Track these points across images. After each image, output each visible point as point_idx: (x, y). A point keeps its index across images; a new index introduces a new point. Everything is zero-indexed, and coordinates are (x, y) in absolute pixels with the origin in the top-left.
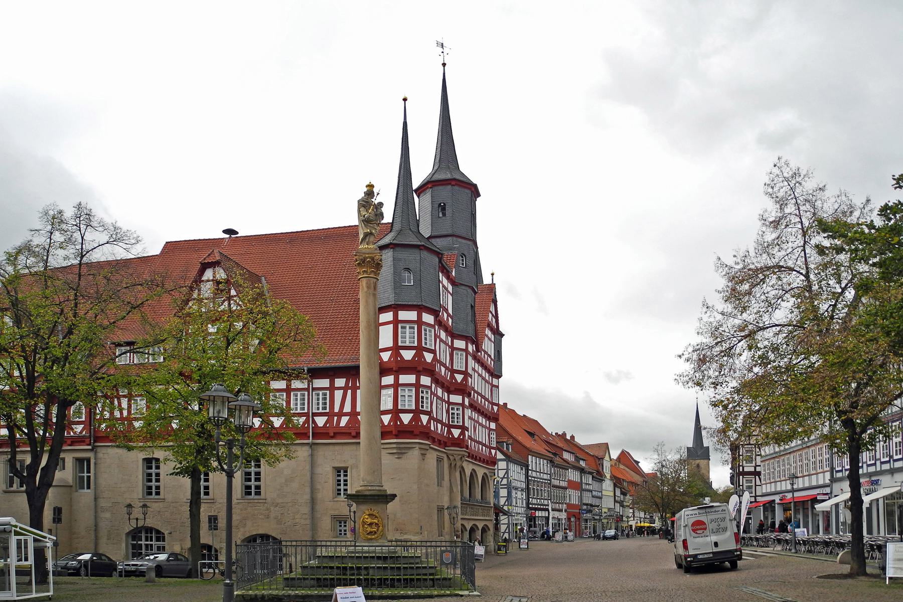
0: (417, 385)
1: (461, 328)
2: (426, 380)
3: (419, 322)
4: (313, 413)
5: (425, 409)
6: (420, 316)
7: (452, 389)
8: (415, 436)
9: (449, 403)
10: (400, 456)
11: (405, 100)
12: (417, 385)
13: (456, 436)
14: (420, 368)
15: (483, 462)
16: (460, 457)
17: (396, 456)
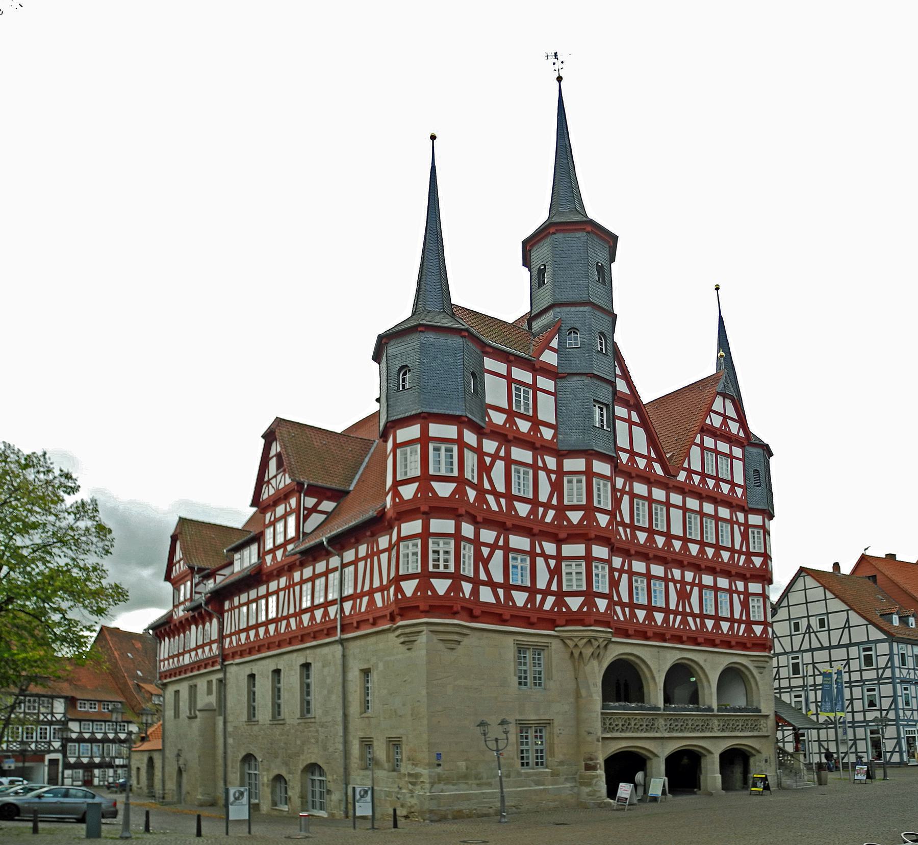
1: (573, 439)
7: (563, 535)
8: (427, 613)
9: (559, 558)
10: (409, 646)
11: (433, 138)
17: (407, 647)
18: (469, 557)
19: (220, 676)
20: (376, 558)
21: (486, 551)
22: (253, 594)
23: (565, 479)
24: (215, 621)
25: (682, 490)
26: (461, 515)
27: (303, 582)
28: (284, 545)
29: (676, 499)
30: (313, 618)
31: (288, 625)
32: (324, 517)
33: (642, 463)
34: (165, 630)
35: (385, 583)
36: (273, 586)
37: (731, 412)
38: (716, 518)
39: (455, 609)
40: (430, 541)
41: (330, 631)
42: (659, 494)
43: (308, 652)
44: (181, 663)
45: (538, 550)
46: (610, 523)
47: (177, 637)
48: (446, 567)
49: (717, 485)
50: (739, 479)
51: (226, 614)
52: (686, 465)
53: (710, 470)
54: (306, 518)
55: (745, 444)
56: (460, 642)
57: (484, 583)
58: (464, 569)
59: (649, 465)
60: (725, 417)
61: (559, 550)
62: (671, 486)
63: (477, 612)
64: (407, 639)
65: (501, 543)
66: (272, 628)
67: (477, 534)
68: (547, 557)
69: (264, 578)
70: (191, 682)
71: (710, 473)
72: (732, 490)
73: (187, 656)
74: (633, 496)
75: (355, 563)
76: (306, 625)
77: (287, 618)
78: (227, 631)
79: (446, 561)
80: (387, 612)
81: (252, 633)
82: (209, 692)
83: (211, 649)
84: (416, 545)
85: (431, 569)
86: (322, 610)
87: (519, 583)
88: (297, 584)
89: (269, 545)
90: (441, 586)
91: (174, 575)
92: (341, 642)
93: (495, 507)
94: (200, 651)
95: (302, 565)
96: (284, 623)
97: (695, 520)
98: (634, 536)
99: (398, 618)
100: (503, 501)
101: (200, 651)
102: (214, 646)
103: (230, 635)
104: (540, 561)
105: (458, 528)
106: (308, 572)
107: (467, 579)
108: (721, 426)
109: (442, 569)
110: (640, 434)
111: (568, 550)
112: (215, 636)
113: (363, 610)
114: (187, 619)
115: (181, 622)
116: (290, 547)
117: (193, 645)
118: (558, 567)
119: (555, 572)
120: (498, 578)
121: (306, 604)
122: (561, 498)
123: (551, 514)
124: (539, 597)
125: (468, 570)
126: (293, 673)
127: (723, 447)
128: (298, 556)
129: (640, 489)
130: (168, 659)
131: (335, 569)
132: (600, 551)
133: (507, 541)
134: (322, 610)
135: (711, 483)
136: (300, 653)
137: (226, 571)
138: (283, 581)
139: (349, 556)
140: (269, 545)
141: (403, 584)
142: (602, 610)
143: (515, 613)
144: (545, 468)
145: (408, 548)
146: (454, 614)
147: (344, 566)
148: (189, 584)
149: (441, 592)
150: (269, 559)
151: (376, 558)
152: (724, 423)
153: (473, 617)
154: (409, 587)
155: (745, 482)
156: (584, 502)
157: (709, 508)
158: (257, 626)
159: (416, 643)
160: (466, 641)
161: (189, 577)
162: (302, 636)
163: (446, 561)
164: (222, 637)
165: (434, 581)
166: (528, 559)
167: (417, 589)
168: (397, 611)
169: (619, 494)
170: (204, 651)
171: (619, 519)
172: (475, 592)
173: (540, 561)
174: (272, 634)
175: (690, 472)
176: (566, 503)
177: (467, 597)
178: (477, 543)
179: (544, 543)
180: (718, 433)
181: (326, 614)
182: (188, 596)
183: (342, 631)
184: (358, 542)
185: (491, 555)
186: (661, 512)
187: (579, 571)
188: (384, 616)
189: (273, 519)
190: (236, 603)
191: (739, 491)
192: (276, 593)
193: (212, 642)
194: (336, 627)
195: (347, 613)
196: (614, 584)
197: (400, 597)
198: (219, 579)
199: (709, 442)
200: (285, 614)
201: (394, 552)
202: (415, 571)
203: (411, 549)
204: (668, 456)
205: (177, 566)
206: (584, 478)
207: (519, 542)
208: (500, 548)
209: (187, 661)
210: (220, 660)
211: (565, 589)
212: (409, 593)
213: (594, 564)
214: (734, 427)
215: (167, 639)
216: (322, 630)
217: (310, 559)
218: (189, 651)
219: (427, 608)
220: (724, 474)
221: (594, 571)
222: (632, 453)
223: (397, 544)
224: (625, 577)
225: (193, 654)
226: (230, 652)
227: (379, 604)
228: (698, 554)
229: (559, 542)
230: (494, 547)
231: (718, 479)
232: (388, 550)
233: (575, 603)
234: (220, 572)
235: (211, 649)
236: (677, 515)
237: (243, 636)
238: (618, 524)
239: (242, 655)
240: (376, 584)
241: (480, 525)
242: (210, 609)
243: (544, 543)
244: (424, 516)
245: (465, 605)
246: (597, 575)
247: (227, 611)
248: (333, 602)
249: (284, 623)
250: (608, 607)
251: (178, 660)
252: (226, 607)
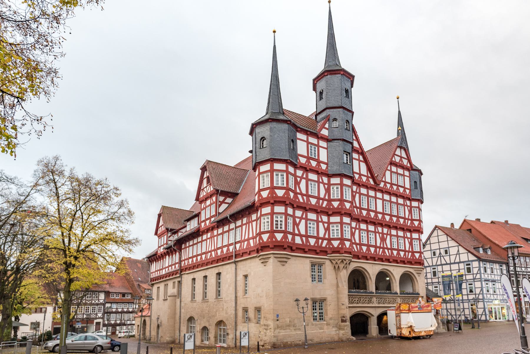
3: (272, 171)
4: (235, 242)
7: (330, 213)
8: (272, 249)
9: (329, 223)
10: (265, 264)
12: (272, 213)
13: (336, 246)
14: (272, 201)
15: (403, 262)
16: (340, 261)
18: (291, 223)
19: (179, 279)
20: (250, 224)
21: (298, 220)
22: (195, 241)
23: (331, 187)
24: (177, 253)
25: (382, 191)
26: (287, 205)
27: (218, 235)
28: (210, 218)
29: (379, 195)
30: (222, 251)
31: (211, 255)
32: (227, 205)
33: (364, 179)
34: (154, 258)
35: (254, 235)
36: (205, 237)
37: (404, 155)
38: (397, 204)
39: (285, 247)
40: (274, 216)
41: (230, 258)
42: (372, 193)
43: (220, 267)
44: (161, 274)
45: (320, 220)
46: (350, 207)
47: (159, 262)
48: (281, 228)
49: (398, 189)
50: (407, 186)
51: (183, 250)
52: (384, 180)
53: (395, 181)
54: (220, 206)
55: (410, 169)
56: (286, 262)
57: (297, 235)
58: (289, 228)
59: (368, 180)
60: (401, 157)
61: (329, 219)
62: (377, 189)
63: (294, 248)
64: (264, 261)
65: (304, 217)
66: (204, 256)
67: (294, 213)
68: (323, 223)
69: (201, 233)
70: (166, 283)
71: (394, 183)
72: (404, 191)
73: (164, 270)
74: (360, 194)
75: (241, 226)
76: (219, 255)
77: (211, 252)
78: (183, 258)
79: (281, 225)
80: (255, 249)
81: (195, 259)
82: (174, 287)
83: (175, 267)
84: (268, 218)
85: (275, 229)
86: (227, 248)
87: (312, 234)
88: (215, 236)
89: (203, 218)
90: (279, 236)
91: (159, 232)
92: (235, 262)
93: (301, 201)
94: (170, 268)
95: (218, 227)
96: (209, 254)
97: (388, 205)
98: (361, 213)
99: (260, 251)
100: (305, 197)
101: (170, 268)
102: (177, 265)
103: (184, 260)
104: (321, 224)
105: (286, 210)
106: (220, 231)
107: (290, 233)
108: (399, 162)
109: (279, 229)
110: (363, 166)
111: (333, 219)
112: (177, 261)
113: (245, 247)
114: (164, 253)
115: (162, 254)
116: (213, 219)
117: (167, 265)
118: (328, 227)
119: (327, 229)
120: (303, 232)
121: (220, 245)
122: (329, 196)
123: (325, 203)
124: (320, 241)
125: (290, 229)
126: (213, 277)
127: (400, 171)
128: (216, 223)
129: (364, 191)
130: (155, 272)
131: (233, 229)
132: (347, 220)
133: (306, 216)
134: (227, 248)
135: (395, 187)
136: (216, 268)
137: (183, 230)
138: (209, 235)
139: (239, 223)
140: (203, 218)
141: (263, 236)
142: (348, 246)
143: (310, 248)
144: (323, 183)
145: (265, 219)
146: (285, 249)
147: (236, 227)
148: (166, 236)
149: (279, 239)
150: (203, 224)
151: (250, 224)
152: (401, 160)
153: (292, 250)
154: (265, 237)
155: (410, 187)
156: (339, 198)
157: (394, 199)
158: (197, 256)
160: (289, 261)
161: (166, 233)
162: (217, 260)
163: (281, 225)
164: (180, 261)
166: (316, 223)
168: (260, 248)
169: (354, 193)
170: (172, 268)
171: (354, 205)
172: (293, 239)
173: (321, 224)
174: (204, 259)
175: (385, 182)
176: (332, 198)
177: (290, 241)
178: (294, 216)
179: (322, 216)
180: (398, 165)
181: (228, 250)
182: (165, 242)
183: (235, 257)
184: (243, 217)
185: (300, 222)
186: (372, 201)
187: (337, 228)
188: (255, 250)
189: (205, 206)
190: (188, 245)
191: (408, 191)
192: (206, 240)
193: (176, 263)
194: (233, 256)
195: (238, 249)
196: (353, 234)
197: (261, 241)
198: (180, 234)
199: (394, 169)
200: (210, 250)
201: (259, 221)
202: (268, 230)
203: (266, 220)
204: (376, 175)
205: (161, 228)
206: (339, 187)
207: (312, 216)
208: (304, 219)
209: (164, 273)
210: (179, 272)
211: (331, 237)
212: (265, 240)
213: (344, 225)
214: (405, 162)
215: (154, 262)
216: (227, 257)
217: (222, 224)
218: (165, 268)
219: (273, 247)
220: (401, 183)
221: (344, 229)
222: (360, 175)
223: (260, 218)
224: (357, 231)
225: (167, 269)
226: (184, 268)
227: (252, 245)
228: (389, 220)
229: (329, 215)
230: (301, 218)
231: (398, 186)
232: (256, 220)
233: (336, 244)
234: (180, 231)
235: (175, 267)
236: (379, 202)
237: (190, 260)
238: (354, 207)
239: (189, 270)
240: (251, 236)
241: (295, 209)
242: (175, 248)
243: (322, 216)
245: (289, 245)
246: (345, 231)
247: (183, 249)
248: (232, 244)
249: (209, 254)
250: (350, 245)
251: (160, 273)
252: (183, 247)
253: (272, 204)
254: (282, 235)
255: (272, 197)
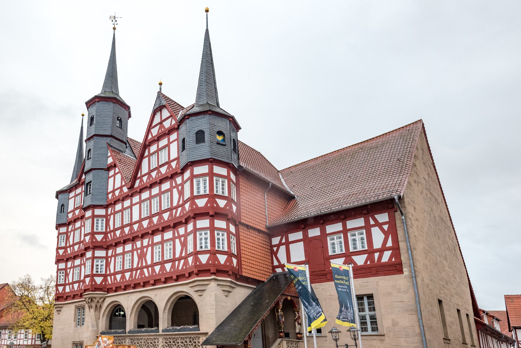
0: (212, 229)
2: (220, 224)
5: (221, 249)
6: (211, 170)
105: (228, 226)
149: (222, 262)
159: (205, 291)
165: (218, 256)
167: (209, 260)
219: (215, 272)
244: (211, 218)
253: (212, 216)
254: (225, 257)
255: (212, 207)
